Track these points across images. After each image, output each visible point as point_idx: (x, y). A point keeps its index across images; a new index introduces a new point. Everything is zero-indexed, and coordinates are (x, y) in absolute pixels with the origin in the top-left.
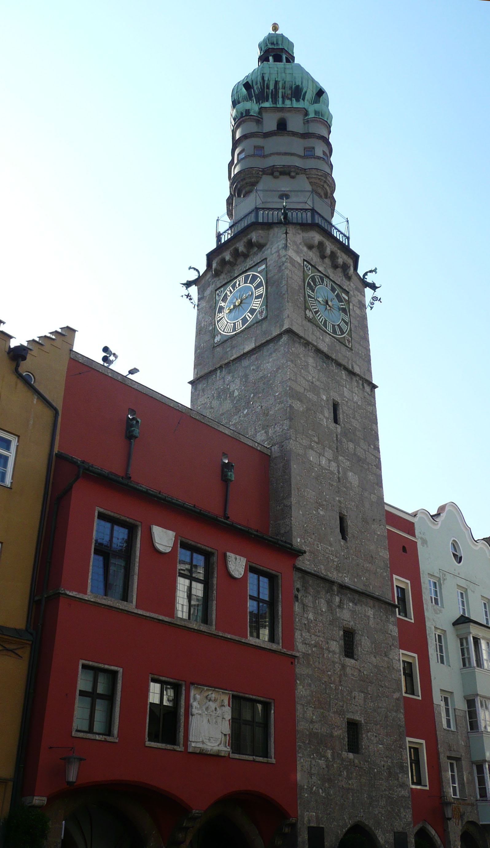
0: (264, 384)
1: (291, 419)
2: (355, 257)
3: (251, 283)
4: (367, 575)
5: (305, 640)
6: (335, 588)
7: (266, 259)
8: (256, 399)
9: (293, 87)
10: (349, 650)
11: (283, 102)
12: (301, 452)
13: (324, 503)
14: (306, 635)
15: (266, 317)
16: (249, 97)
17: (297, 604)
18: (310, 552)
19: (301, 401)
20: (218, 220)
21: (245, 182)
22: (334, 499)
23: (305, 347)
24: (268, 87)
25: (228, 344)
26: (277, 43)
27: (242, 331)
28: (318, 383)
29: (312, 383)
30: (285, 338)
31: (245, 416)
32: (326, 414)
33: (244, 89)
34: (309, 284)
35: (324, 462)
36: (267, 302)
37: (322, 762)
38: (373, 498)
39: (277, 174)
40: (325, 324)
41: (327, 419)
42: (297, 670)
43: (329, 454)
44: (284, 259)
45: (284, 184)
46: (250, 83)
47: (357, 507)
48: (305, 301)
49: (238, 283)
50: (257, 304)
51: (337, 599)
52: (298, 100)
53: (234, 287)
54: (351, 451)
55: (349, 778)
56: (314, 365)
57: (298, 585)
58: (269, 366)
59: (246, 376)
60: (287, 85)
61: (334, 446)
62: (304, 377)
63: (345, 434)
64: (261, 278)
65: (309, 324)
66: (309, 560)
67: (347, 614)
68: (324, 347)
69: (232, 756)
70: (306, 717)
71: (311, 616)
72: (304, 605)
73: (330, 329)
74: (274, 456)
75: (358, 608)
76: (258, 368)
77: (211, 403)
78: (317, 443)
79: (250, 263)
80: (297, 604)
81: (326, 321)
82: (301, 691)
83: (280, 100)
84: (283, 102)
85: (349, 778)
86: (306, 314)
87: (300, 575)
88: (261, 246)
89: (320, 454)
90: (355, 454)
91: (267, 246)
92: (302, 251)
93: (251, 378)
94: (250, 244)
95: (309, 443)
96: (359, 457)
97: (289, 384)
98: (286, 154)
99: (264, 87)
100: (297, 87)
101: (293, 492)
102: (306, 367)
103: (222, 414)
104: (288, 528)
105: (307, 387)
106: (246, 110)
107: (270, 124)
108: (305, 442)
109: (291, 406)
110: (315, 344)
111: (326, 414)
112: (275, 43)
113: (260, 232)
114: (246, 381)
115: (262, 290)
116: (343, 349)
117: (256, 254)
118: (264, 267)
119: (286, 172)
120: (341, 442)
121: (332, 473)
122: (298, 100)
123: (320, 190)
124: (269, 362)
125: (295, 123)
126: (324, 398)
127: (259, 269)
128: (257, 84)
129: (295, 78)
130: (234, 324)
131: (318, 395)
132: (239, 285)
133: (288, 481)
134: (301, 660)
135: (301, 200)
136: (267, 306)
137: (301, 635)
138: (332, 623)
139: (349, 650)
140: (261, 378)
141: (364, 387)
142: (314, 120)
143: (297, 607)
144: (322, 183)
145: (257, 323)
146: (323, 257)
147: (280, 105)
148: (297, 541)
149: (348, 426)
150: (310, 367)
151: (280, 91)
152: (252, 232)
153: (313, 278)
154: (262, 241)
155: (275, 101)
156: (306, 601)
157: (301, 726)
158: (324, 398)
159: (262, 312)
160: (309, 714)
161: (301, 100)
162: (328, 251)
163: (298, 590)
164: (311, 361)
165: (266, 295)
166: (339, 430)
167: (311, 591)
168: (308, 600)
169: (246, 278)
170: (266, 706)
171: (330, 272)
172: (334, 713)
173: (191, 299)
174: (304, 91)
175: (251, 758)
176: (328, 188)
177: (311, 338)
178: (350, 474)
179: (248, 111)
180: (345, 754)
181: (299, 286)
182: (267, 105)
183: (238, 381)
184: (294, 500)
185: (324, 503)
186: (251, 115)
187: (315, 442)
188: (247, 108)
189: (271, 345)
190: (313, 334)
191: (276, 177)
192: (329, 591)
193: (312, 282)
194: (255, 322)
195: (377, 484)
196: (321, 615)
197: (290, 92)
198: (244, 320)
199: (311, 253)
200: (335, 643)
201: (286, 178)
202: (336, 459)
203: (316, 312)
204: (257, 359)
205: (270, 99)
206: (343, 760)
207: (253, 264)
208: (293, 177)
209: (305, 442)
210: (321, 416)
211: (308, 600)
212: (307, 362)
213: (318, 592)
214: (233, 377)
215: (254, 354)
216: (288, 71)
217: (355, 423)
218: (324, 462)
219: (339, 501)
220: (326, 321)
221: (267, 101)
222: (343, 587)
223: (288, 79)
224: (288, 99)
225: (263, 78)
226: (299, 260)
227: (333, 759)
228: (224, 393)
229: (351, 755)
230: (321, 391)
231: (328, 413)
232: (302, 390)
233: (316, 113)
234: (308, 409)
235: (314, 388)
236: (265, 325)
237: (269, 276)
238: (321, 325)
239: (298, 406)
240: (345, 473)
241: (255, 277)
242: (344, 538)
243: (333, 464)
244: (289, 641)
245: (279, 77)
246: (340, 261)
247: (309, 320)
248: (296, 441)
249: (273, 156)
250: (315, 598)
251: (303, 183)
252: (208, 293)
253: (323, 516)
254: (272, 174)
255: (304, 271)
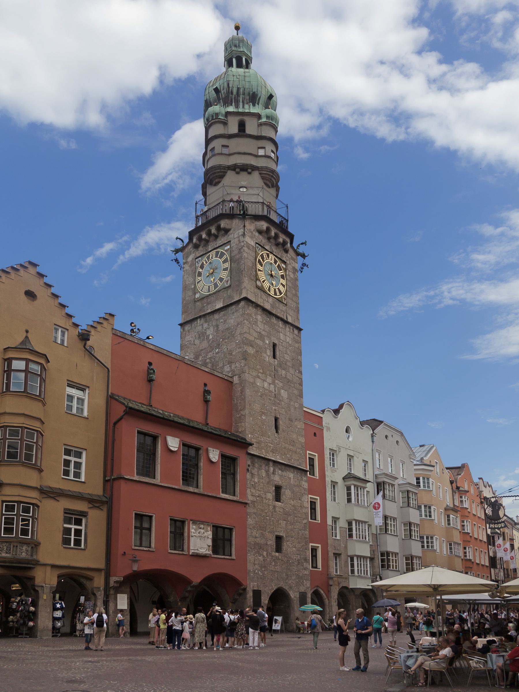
0: (229, 333)
1: (245, 359)
2: (291, 237)
3: (220, 258)
4: (290, 453)
5: (252, 493)
6: (271, 464)
7: (230, 241)
8: (223, 342)
9: (251, 93)
10: (278, 498)
11: (243, 107)
12: (252, 380)
13: (266, 411)
14: (253, 491)
15: (230, 286)
16: (218, 100)
17: (248, 474)
18: (256, 442)
19: (252, 346)
20: (196, 204)
21: (214, 175)
22: (272, 408)
23: (256, 308)
24: (232, 93)
25: (205, 300)
26: (239, 46)
27: (214, 293)
28: (263, 333)
29: (260, 333)
30: (242, 303)
31: (217, 353)
32: (268, 354)
33: (213, 91)
34: (259, 260)
35: (266, 385)
36: (231, 275)
37: (261, 558)
38: (297, 405)
39: (238, 170)
40: (269, 290)
41: (269, 356)
42: (248, 510)
43: (269, 380)
44: (242, 244)
45: (243, 179)
46: (219, 88)
47: (286, 412)
48: (257, 275)
49: (211, 256)
50: (224, 275)
51: (272, 469)
52: (254, 105)
53: (208, 258)
54: (284, 376)
55: (275, 565)
56: (262, 320)
57: (249, 463)
58: (232, 321)
59: (217, 326)
60: (246, 92)
61: (273, 374)
62: (254, 330)
63: (280, 365)
64: (227, 256)
65: (258, 291)
66: (256, 447)
67: (277, 479)
68: (268, 307)
69: (213, 556)
70: (253, 535)
71: (256, 480)
72: (252, 474)
73: (272, 293)
74: (235, 382)
75: (284, 473)
76: (225, 321)
77: (194, 341)
78: (262, 373)
79: (219, 242)
80: (248, 474)
81: (270, 287)
82: (250, 521)
83: (241, 104)
84: (243, 107)
85: (275, 565)
86: (256, 284)
87: (250, 457)
88: (227, 231)
89: (264, 381)
90: (286, 378)
91: (231, 232)
92: (255, 236)
93: (221, 328)
94: (219, 228)
95: (257, 374)
96: (288, 379)
97: (245, 335)
98: (245, 154)
99: (229, 92)
100: (254, 93)
101: (247, 407)
102: (256, 322)
103: (202, 350)
104: (243, 429)
105: (257, 337)
106: (216, 114)
107: (234, 129)
108: (254, 374)
109: (246, 351)
110: (262, 304)
111: (268, 354)
112: (237, 45)
113: (226, 220)
114: (217, 329)
115: (227, 265)
116: (281, 305)
117: (223, 235)
118: (228, 247)
119: (244, 169)
120: (277, 371)
121: (270, 392)
122: (254, 105)
123: (268, 183)
124: (232, 318)
125: (251, 128)
126: (267, 342)
127: (226, 248)
128: (224, 89)
129: (252, 86)
130: (209, 286)
131: (263, 341)
132: (212, 257)
133: (244, 399)
134: (251, 505)
135: (255, 192)
136: (231, 277)
137: (250, 491)
138: (268, 483)
139: (278, 498)
140: (227, 329)
141: (293, 331)
142: (265, 124)
143: (248, 476)
144: (270, 177)
145: (224, 288)
146: (269, 239)
147: (241, 110)
148: (249, 437)
149: (282, 359)
150: (259, 323)
151: (241, 96)
152: (221, 220)
153: (262, 256)
154: (228, 227)
155: (237, 107)
156: (253, 472)
157: (250, 540)
158: (267, 342)
159: (228, 281)
160: (254, 533)
161: (256, 105)
162: (273, 234)
163: (249, 466)
164: (259, 317)
165: (231, 269)
166: (276, 363)
167: (256, 465)
168: (255, 471)
169: (217, 253)
170: (231, 530)
171: (274, 249)
172: (268, 532)
173: (178, 263)
174: (259, 97)
175: (223, 557)
176: (274, 181)
177: (260, 302)
178: (282, 391)
179: (217, 114)
180: (274, 554)
181: (253, 263)
182: (231, 109)
183: (212, 329)
184: (247, 412)
185: (266, 411)
186: (220, 119)
187: (261, 373)
188: (216, 112)
189: (234, 307)
190: (261, 298)
191: (238, 173)
192: (267, 465)
193: (262, 258)
194: (222, 287)
195: (299, 396)
196: (262, 479)
197: (248, 98)
198: (216, 285)
199: (261, 237)
200: (270, 494)
201: (244, 174)
202: (273, 383)
203: (264, 281)
204: (224, 315)
205: (234, 104)
206: (272, 556)
207: (222, 244)
208: (250, 173)
209: (254, 374)
210: (265, 355)
211: (255, 471)
212: (257, 319)
213: (261, 466)
214: (209, 325)
215: (222, 311)
216: (247, 79)
217: (287, 357)
218: (266, 385)
219: (275, 409)
220: (270, 287)
221: (231, 105)
222: (275, 462)
223: (247, 87)
224: (247, 103)
225: (228, 85)
226: (253, 243)
227: (267, 554)
228: (202, 335)
229: (277, 554)
230: (266, 338)
231: (269, 352)
232: (253, 339)
233: (268, 117)
234: (257, 351)
235: (261, 337)
236: (230, 291)
237: (232, 255)
238: (267, 290)
239: (251, 350)
240: (279, 391)
241: (222, 254)
242: (277, 432)
243: (272, 386)
244: (244, 493)
245: (241, 84)
246: (281, 240)
247: (258, 287)
248: (249, 374)
249: (236, 156)
250: (259, 469)
251: (256, 178)
252: (190, 259)
253: (265, 420)
254: (234, 170)
255: (256, 251)
